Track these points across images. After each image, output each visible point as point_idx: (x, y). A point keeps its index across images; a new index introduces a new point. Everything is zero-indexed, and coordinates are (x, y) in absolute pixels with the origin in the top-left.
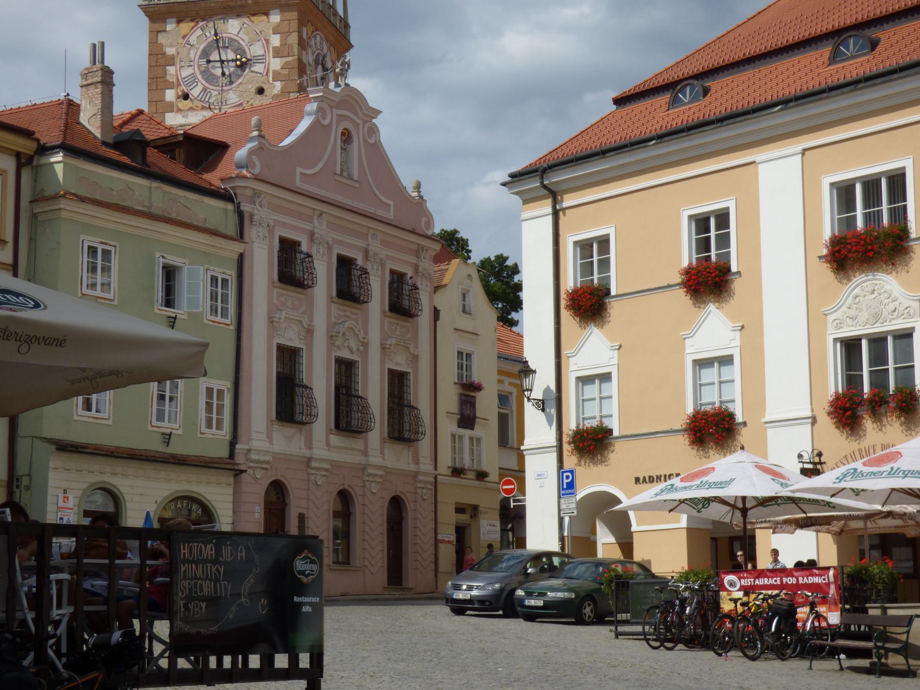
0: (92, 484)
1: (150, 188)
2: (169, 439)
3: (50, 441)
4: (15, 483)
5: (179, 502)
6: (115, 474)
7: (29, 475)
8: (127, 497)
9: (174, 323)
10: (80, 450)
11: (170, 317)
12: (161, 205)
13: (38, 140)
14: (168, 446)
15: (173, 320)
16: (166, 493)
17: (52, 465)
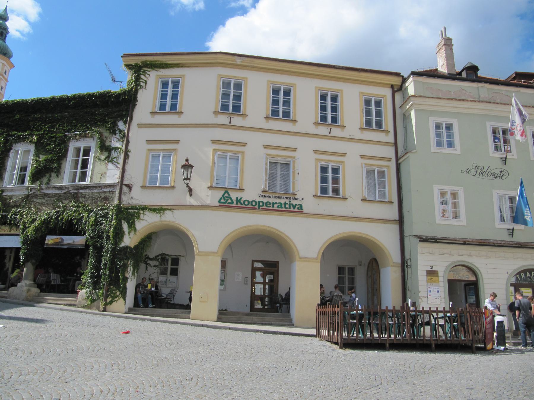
0: (453, 262)
1: (478, 88)
2: (513, 233)
3: (417, 236)
4: (406, 265)
5: (528, 273)
6: (471, 256)
7: (410, 259)
8: (482, 270)
9: (506, 161)
10: (438, 241)
11: (502, 158)
12: (487, 96)
13: (403, 76)
14: (512, 237)
15: (504, 159)
16: (516, 267)
17: (419, 250)
